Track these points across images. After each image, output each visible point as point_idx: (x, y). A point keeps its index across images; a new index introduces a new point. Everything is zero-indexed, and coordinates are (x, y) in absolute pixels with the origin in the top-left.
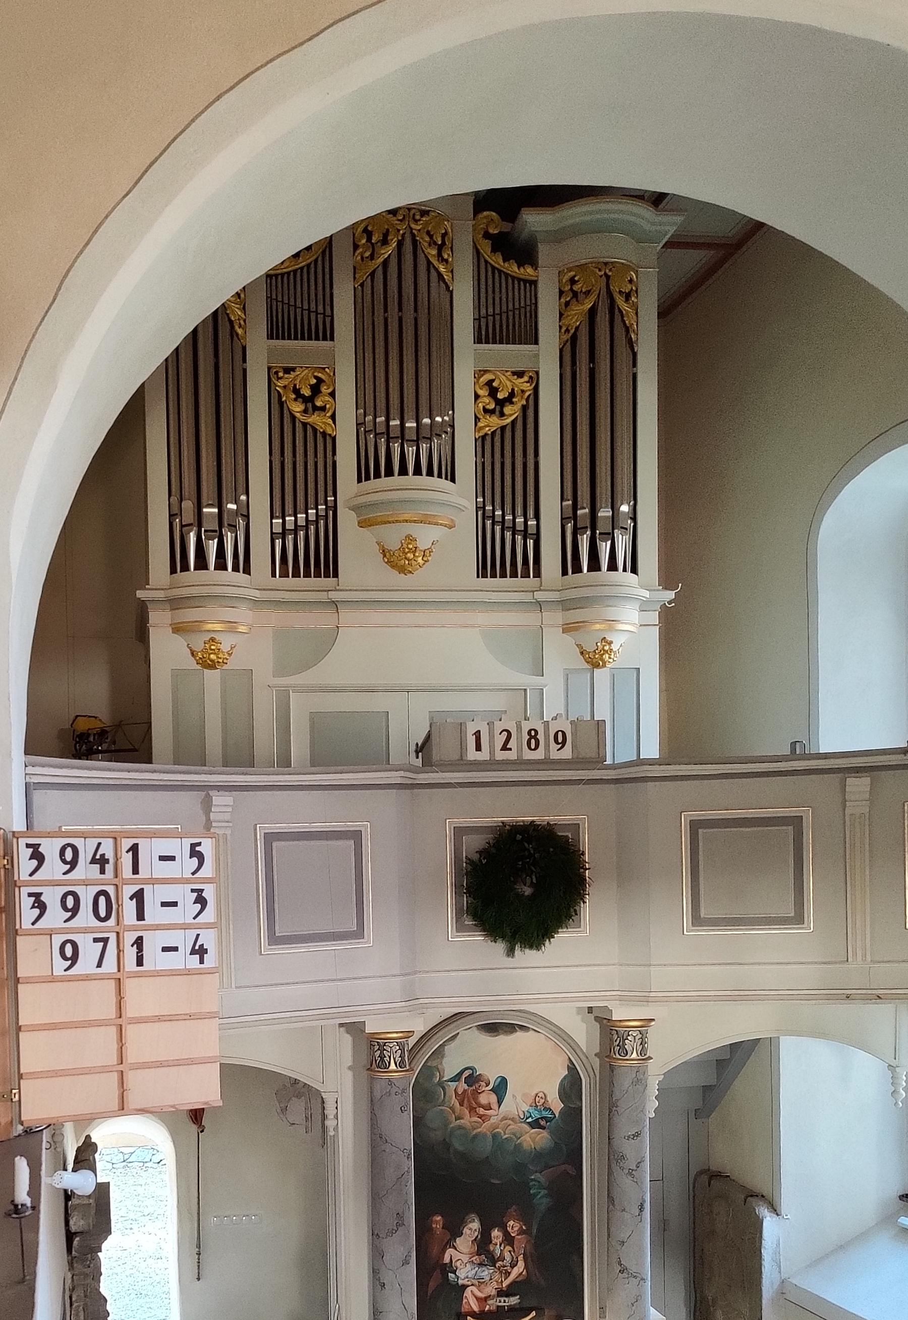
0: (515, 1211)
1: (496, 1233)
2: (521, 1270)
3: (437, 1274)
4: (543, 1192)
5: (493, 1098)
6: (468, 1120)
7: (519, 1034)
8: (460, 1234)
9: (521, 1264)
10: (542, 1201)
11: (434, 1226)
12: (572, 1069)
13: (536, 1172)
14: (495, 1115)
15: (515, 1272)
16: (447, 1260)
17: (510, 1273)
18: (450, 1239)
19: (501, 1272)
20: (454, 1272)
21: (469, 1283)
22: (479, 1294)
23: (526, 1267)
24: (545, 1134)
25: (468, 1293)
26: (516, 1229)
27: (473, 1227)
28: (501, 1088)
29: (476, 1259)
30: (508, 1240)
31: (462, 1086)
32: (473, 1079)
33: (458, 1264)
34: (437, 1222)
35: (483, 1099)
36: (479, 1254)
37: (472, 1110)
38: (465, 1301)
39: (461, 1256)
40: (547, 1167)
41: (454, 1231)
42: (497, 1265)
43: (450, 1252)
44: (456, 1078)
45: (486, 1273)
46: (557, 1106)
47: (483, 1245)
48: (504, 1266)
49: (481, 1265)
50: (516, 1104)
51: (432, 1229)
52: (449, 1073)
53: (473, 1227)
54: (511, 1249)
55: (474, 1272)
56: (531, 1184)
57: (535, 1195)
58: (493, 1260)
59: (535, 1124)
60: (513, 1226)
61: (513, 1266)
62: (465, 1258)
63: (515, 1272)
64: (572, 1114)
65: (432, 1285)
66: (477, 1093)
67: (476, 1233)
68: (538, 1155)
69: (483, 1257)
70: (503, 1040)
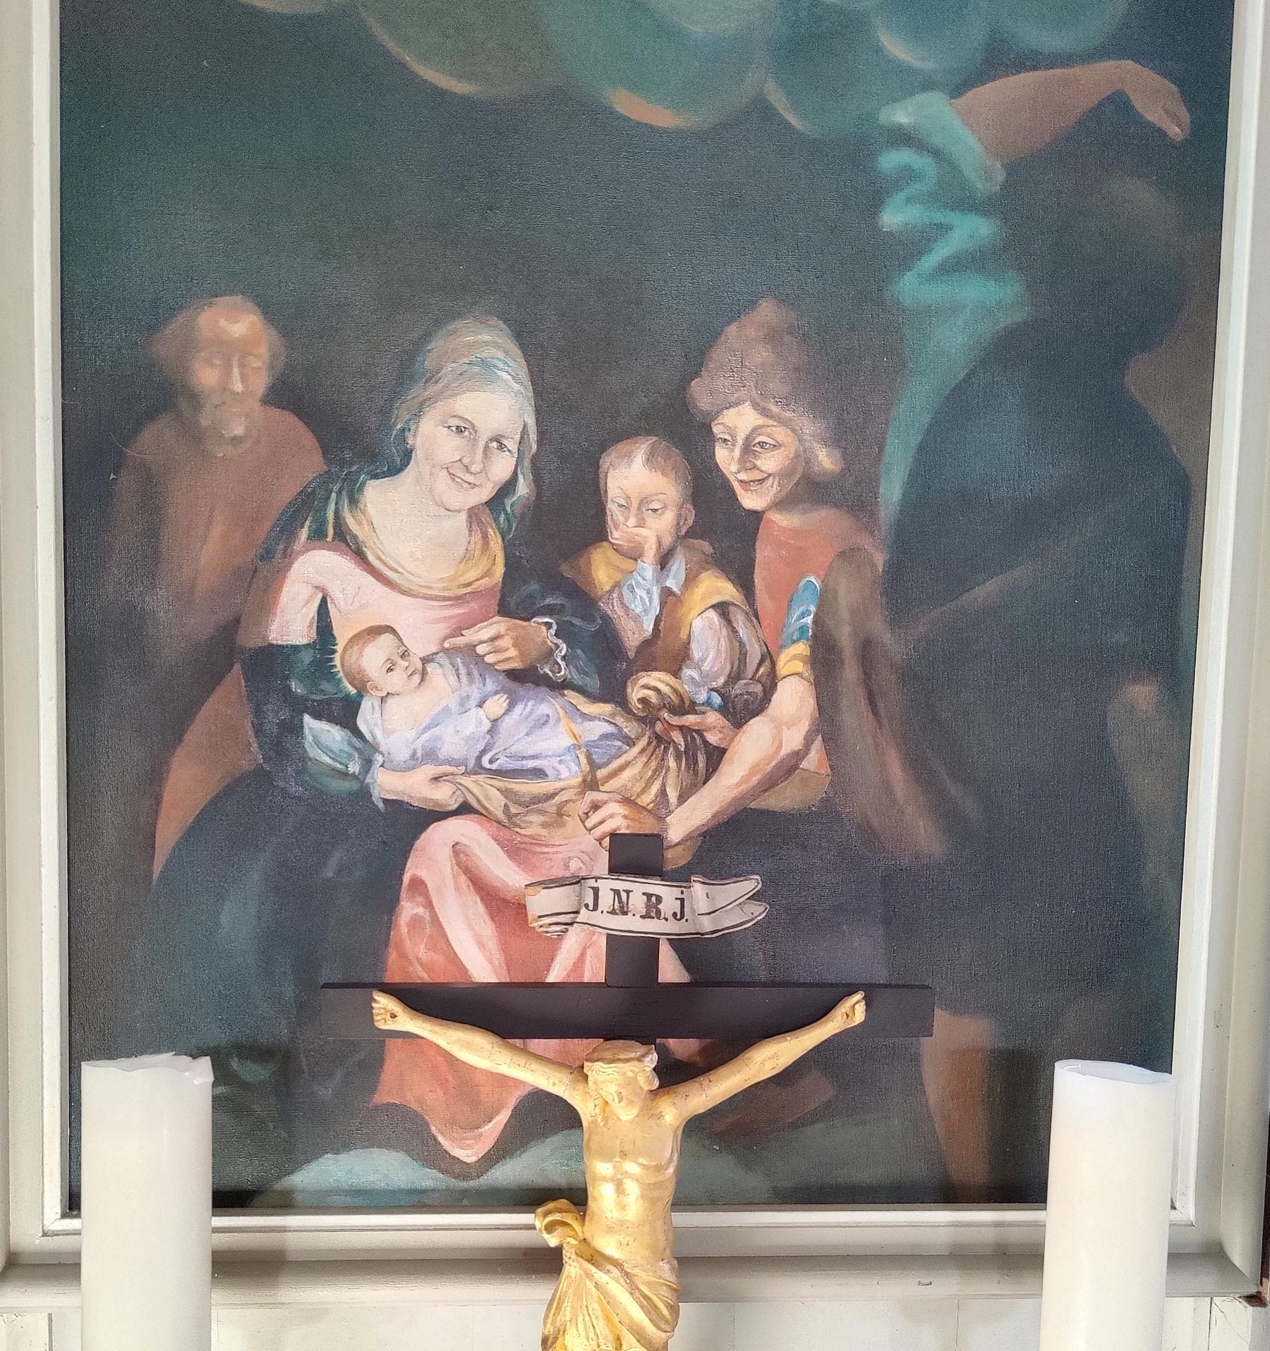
0: (772, 337)
1: (637, 480)
2: (793, 740)
3: (226, 704)
4: (971, 230)
8: (394, 462)
9: (794, 699)
11: (206, 376)
13: (929, 84)
15: (753, 750)
16: (291, 624)
17: (716, 756)
18: (325, 480)
19: (660, 740)
20: (344, 712)
21: (444, 795)
22: (508, 875)
23: (826, 722)
25: (432, 856)
26: (770, 463)
27: (477, 412)
29: (499, 638)
30: (720, 529)
33: (372, 659)
34: (228, 350)
36: (512, 602)
38: (409, 909)
40: (999, 59)
41: (346, 430)
42: (635, 694)
43: (314, 571)
45: (557, 735)
48: (684, 706)
49: (525, 678)
51: (195, 399)
54: (727, 590)
55: (475, 723)
56: (891, 160)
57: (912, 246)
58: (606, 663)
60: (760, 435)
61: (740, 711)
62: (420, 626)
63: (753, 750)
65: (188, 785)
67: (502, 467)
69: (542, 630)
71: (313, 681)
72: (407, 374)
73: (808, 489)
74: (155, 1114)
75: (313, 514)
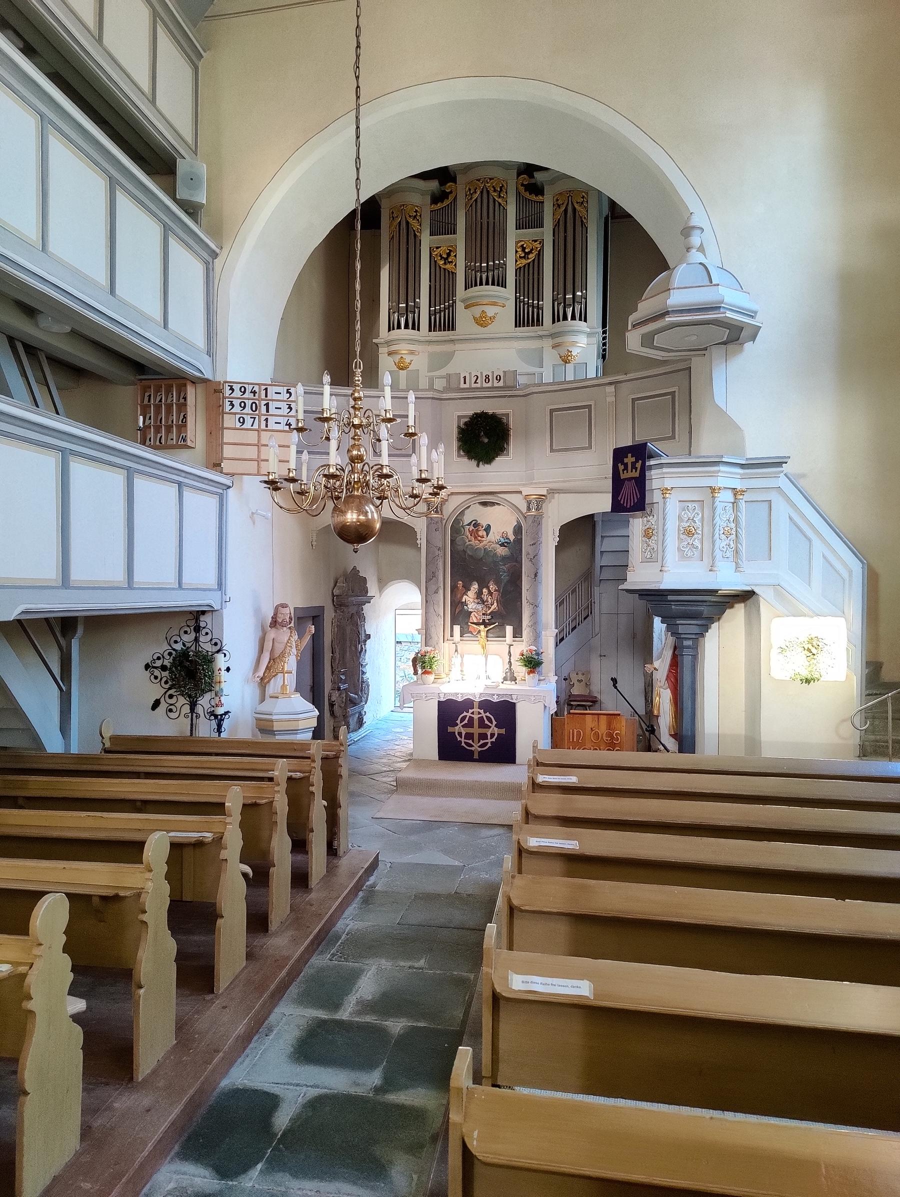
1: (485, 590)
5: (485, 533)
6: (474, 542)
7: (496, 506)
10: (505, 577)
12: (518, 522)
14: (486, 541)
15: (493, 607)
24: (507, 549)
25: (472, 615)
28: (488, 529)
30: (490, 593)
31: (472, 528)
32: (476, 525)
35: (480, 533)
37: (475, 538)
39: (470, 598)
41: (467, 588)
43: (465, 597)
44: (469, 524)
45: (480, 607)
46: (512, 538)
47: (479, 594)
50: (495, 536)
52: (466, 522)
53: (475, 586)
58: (483, 602)
59: (502, 545)
62: (471, 600)
64: (518, 541)
66: (478, 531)
68: (504, 558)
70: (489, 509)
71: (465, 604)
72: (471, 585)
73: (496, 590)
74: (457, 629)
75: (465, 594)
